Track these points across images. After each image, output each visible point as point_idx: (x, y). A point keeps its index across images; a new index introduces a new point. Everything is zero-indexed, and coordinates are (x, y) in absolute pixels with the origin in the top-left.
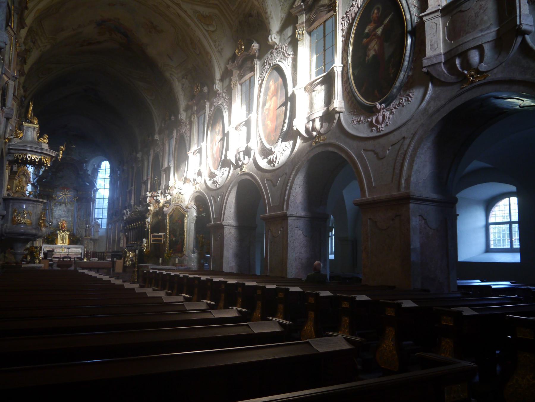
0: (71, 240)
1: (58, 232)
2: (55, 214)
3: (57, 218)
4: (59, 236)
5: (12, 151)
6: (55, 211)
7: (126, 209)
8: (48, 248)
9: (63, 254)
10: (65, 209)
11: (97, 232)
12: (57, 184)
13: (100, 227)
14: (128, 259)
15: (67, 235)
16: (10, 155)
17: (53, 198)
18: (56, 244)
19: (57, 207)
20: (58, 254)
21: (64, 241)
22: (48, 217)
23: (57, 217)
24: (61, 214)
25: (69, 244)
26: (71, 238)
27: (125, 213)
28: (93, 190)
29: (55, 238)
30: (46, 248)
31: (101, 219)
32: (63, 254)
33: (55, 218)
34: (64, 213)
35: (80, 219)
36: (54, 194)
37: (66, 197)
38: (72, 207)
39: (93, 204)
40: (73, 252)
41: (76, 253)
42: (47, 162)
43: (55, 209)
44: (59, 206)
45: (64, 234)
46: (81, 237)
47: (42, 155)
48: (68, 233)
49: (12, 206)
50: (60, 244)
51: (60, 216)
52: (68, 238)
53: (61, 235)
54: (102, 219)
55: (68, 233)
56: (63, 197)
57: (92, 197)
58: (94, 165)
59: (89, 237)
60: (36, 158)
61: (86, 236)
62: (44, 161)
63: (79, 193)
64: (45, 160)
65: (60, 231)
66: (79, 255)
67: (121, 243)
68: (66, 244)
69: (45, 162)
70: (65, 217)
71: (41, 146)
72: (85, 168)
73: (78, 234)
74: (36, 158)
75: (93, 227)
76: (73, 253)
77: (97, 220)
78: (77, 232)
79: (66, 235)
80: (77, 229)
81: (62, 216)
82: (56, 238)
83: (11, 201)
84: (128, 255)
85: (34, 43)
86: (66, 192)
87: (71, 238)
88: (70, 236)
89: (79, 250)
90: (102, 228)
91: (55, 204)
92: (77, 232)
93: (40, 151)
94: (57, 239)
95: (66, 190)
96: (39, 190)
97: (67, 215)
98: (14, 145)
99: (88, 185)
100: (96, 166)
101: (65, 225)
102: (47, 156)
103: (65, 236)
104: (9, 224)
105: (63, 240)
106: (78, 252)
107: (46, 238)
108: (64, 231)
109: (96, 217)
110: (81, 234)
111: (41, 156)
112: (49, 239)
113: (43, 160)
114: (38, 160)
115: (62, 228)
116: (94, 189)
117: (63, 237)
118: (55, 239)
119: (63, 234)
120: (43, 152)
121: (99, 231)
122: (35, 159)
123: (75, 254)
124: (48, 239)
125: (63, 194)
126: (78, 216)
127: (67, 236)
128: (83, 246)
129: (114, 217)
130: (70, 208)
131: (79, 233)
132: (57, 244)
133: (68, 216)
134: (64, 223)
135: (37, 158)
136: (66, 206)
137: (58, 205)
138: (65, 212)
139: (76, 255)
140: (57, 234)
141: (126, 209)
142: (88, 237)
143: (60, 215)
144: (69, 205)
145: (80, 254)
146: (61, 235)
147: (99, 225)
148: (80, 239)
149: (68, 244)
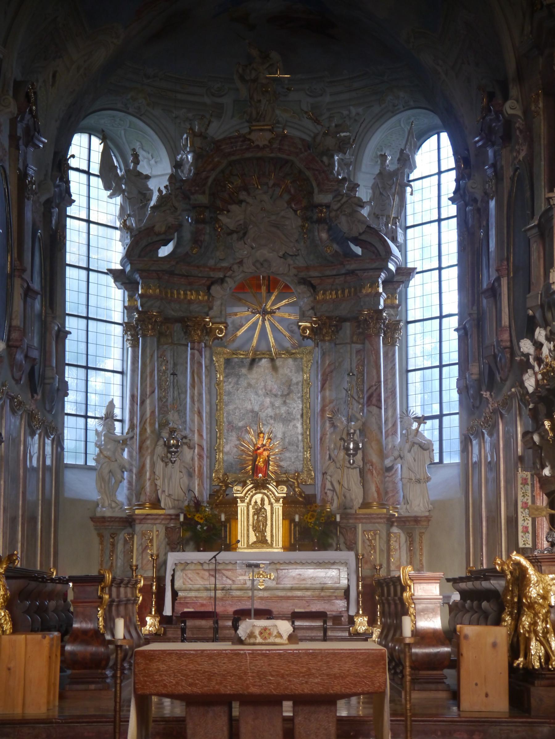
0: (296, 525)
1: (237, 491)
2: (231, 407)
3: (240, 428)
4: (241, 505)
6: (229, 394)
7: (530, 335)
8: (192, 567)
9: (261, 598)
10: (272, 384)
11: (418, 481)
12: (225, 264)
13: (431, 458)
14: (534, 624)
15: (277, 500)
17: (209, 332)
18: (230, 547)
19: (239, 376)
20: (240, 599)
21: (268, 534)
22: (193, 421)
23: (241, 424)
24: (256, 408)
25: (290, 547)
26: (297, 518)
27: (527, 355)
28: (383, 275)
29: (223, 518)
30: (183, 570)
31: (437, 421)
32: (261, 594)
33: (232, 427)
34: (268, 400)
35: (333, 425)
36: (211, 313)
37: (267, 324)
38: (300, 369)
39: (390, 343)
40: (308, 583)
41: (322, 589)
43: (228, 387)
44: (244, 371)
45: (262, 500)
46: (344, 508)
48: (282, 491)
50: (249, 546)
51: (255, 415)
52: (281, 518)
53: (249, 504)
54: (440, 417)
55: (282, 491)
56: (255, 324)
57: (380, 308)
58: (384, 157)
59: (382, 505)
61: (366, 505)
63: (320, 297)
65: (244, 484)
66: (337, 598)
67: (520, 529)
68: (271, 546)
70: (277, 418)
72: (339, 174)
73: (330, 494)
75: (400, 457)
76: (307, 589)
77: (415, 425)
78: (324, 486)
79: (270, 503)
80: (324, 474)
81: (262, 415)
82: (228, 520)
84: (533, 592)
86: (269, 298)
87: (297, 518)
88: (288, 502)
89: (333, 573)
90: (446, 461)
91: (228, 362)
92: (324, 486)
94: (233, 524)
95: (264, 289)
96: (141, 296)
97: (283, 410)
99: (357, 256)
100: (389, 158)
101: (266, 453)
103: (267, 507)
105: (259, 528)
106: (330, 583)
107: (182, 518)
108: (260, 486)
109: (416, 410)
110: (345, 497)
112: (199, 526)
115: (256, 470)
116: (389, 270)
117: (259, 511)
118: (224, 525)
119: (258, 497)
121: (428, 479)
123: (317, 593)
124: (189, 524)
125: (254, 313)
126: (323, 410)
127: (279, 507)
128: (352, 554)
129: (486, 394)
130: (296, 378)
131: (334, 490)
132: (235, 549)
133: (289, 413)
134: (263, 445)
136: (275, 368)
137: (241, 363)
138: (276, 396)
139: (320, 598)
140: (234, 501)
141: (530, 335)
142: (375, 509)
143: (252, 411)
144: (290, 361)
145: (342, 593)
146: (249, 504)
147: (426, 447)
148: (338, 518)
149: (284, 548)
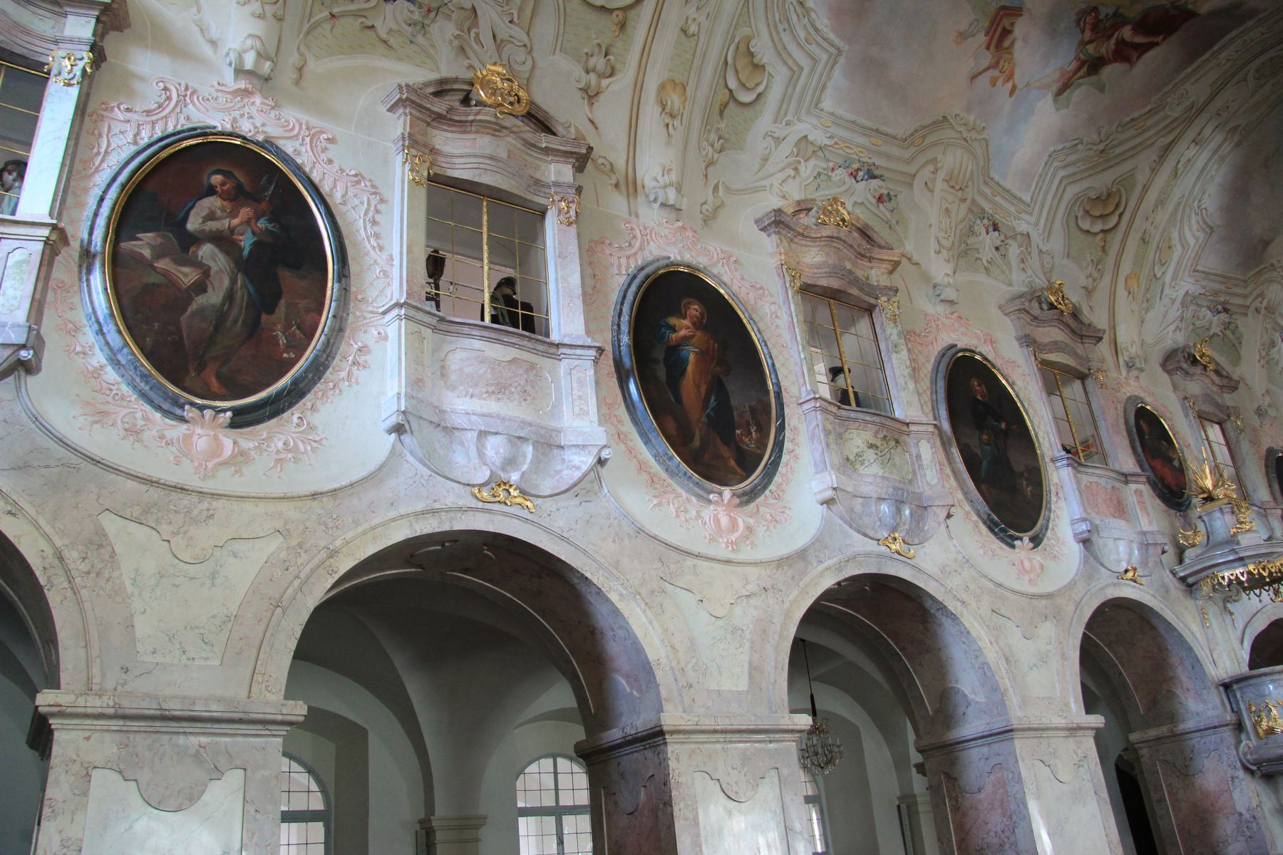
5: (1190, 580)
16: (1195, 587)
42: (1273, 570)
47: (1247, 561)
49: (1242, 697)
60: (1261, 571)
62: (1259, 573)
64: (1264, 569)
69: (1265, 574)
71: (1238, 543)
74: (1239, 575)
83: (1235, 687)
85: (1226, 310)
93: (1231, 558)
98: (1190, 565)
102: (1261, 560)
104: (1254, 742)
111: (1245, 565)
113: (1255, 572)
114: (1245, 575)
120: (1242, 555)
122: (1237, 577)
135: (1242, 574)
